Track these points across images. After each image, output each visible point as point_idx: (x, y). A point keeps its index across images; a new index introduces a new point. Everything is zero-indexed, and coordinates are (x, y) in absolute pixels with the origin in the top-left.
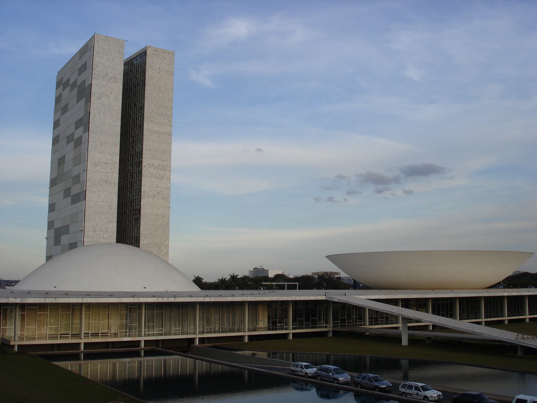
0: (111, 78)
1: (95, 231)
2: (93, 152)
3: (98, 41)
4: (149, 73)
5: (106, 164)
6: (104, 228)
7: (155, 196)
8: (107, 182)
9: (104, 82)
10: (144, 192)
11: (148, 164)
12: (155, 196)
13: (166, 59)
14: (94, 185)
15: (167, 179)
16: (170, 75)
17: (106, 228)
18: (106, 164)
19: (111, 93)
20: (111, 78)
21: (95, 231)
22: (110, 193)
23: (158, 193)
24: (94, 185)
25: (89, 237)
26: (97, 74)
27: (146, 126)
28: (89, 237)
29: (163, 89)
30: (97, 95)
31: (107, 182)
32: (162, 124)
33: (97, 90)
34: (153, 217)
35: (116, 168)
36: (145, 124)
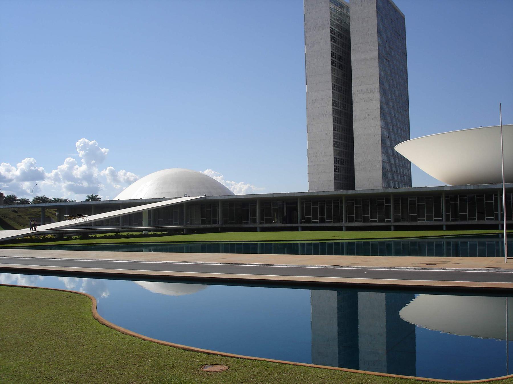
0: (320, 27)
5: (322, 99)
8: (323, 114)
9: (315, 32)
10: (355, 116)
11: (358, 91)
12: (366, 118)
15: (376, 100)
18: (322, 99)
19: (321, 39)
20: (320, 27)
21: (316, 157)
23: (369, 115)
25: (312, 162)
29: (366, 19)
30: (310, 45)
31: (323, 114)
32: (367, 52)
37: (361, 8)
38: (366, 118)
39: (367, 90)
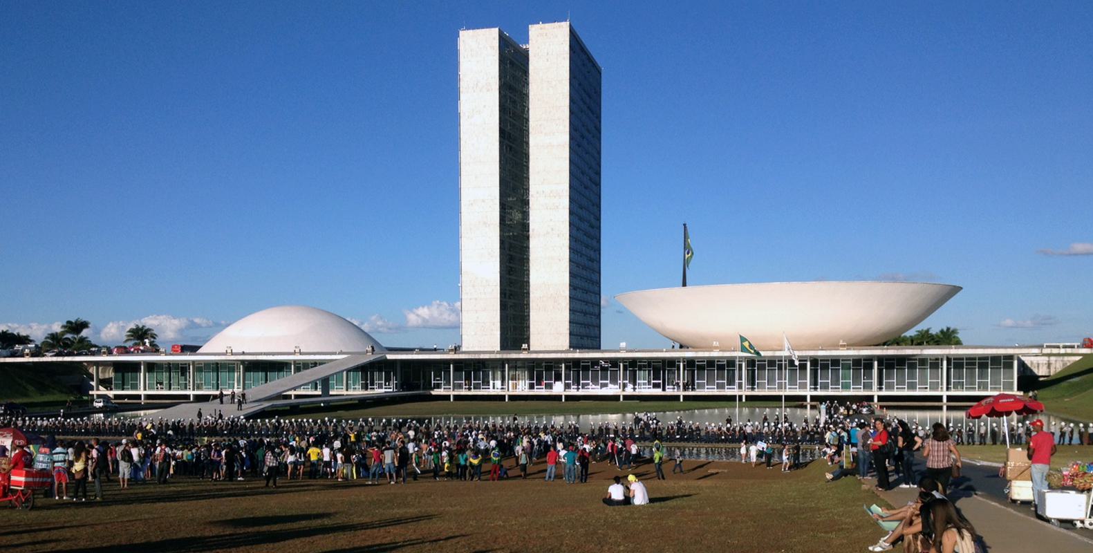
3: (463, 41)
5: (483, 201)
7: (548, 233)
8: (485, 223)
10: (533, 230)
11: (537, 193)
13: (556, 36)
16: (564, 58)
17: (486, 281)
18: (483, 201)
21: (473, 286)
23: (552, 229)
25: (467, 293)
28: (467, 293)
38: (548, 233)
39: (551, 192)
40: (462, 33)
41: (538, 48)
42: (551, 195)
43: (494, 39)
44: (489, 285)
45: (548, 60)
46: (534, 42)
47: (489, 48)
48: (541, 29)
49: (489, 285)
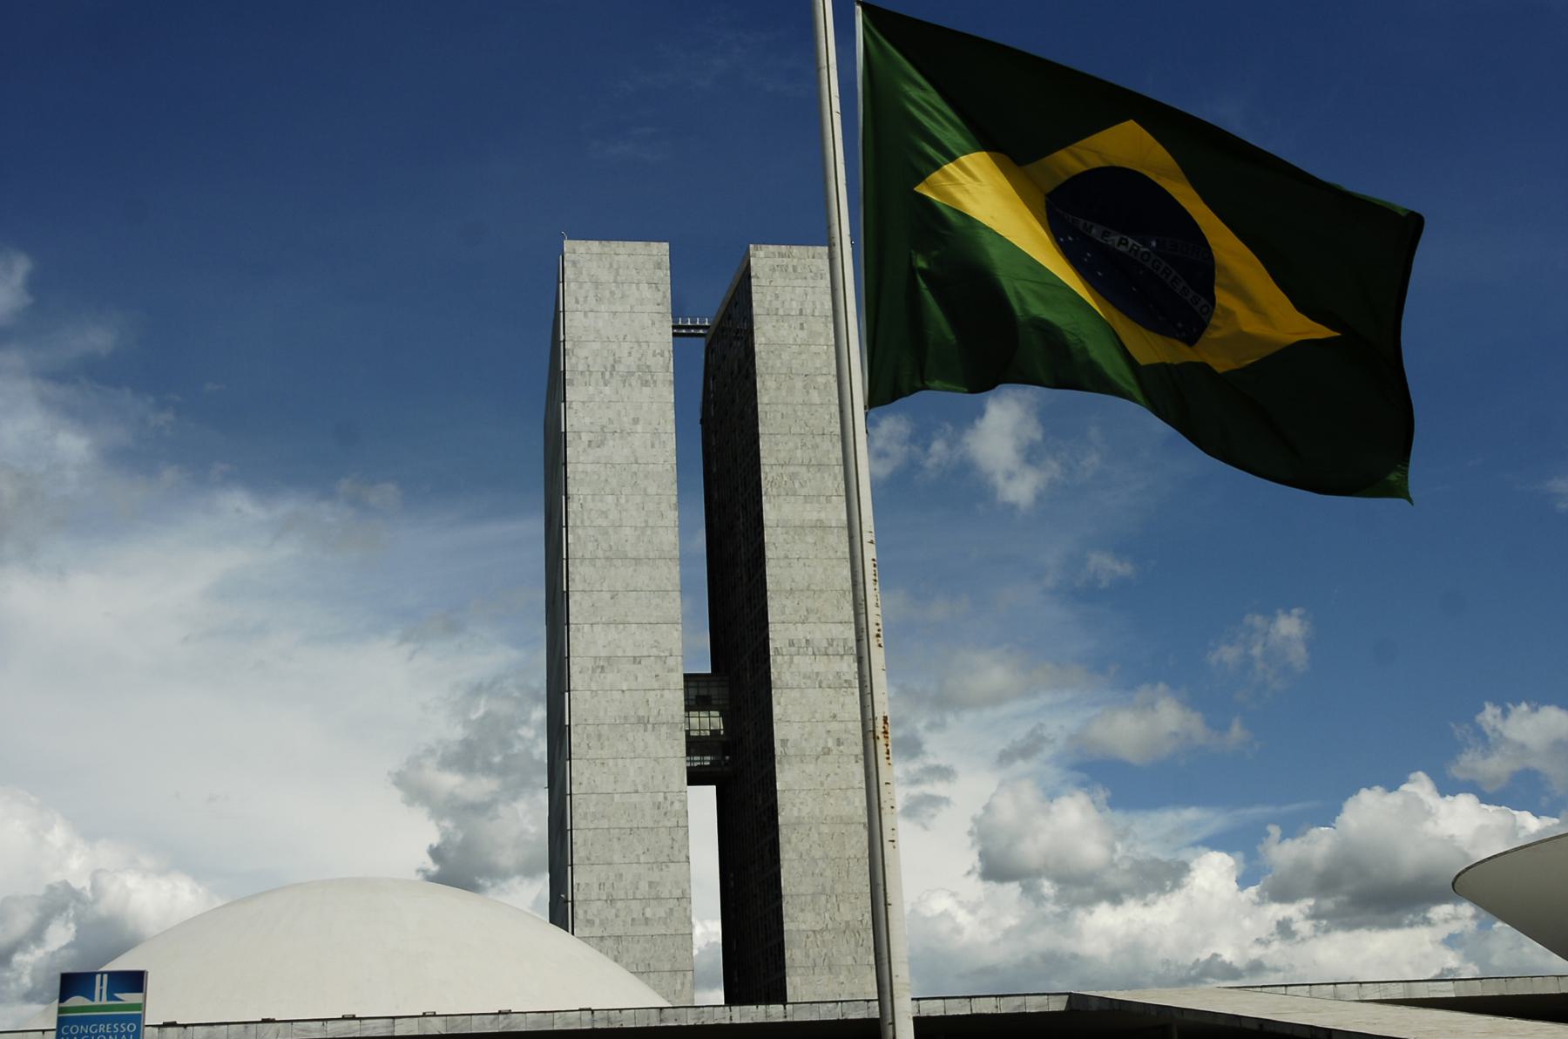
1: (611, 901)
2: (587, 628)
3: (574, 263)
4: (765, 334)
6: (644, 886)
8: (642, 722)
9: (607, 390)
10: (784, 742)
11: (792, 644)
14: (599, 736)
17: (651, 883)
18: (636, 660)
19: (636, 421)
20: (631, 374)
21: (611, 901)
22: (656, 760)
23: (839, 742)
24: (599, 736)
26: (581, 368)
27: (771, 513)
30: (585, 437)
31: (642, 722)
33: (587, 420)
34: (825, 829)
35: (671, 670)
36: (766, 507)
37: (803, 335)
40: (568, 245)
41: (777, 296)
42: (830, 651)
43: (659, 266)
44: (657, 898)
45: (802, 328)
46: (764, 282)
47: (644, 286)
48: (782, 255)
49: (657, 898)
